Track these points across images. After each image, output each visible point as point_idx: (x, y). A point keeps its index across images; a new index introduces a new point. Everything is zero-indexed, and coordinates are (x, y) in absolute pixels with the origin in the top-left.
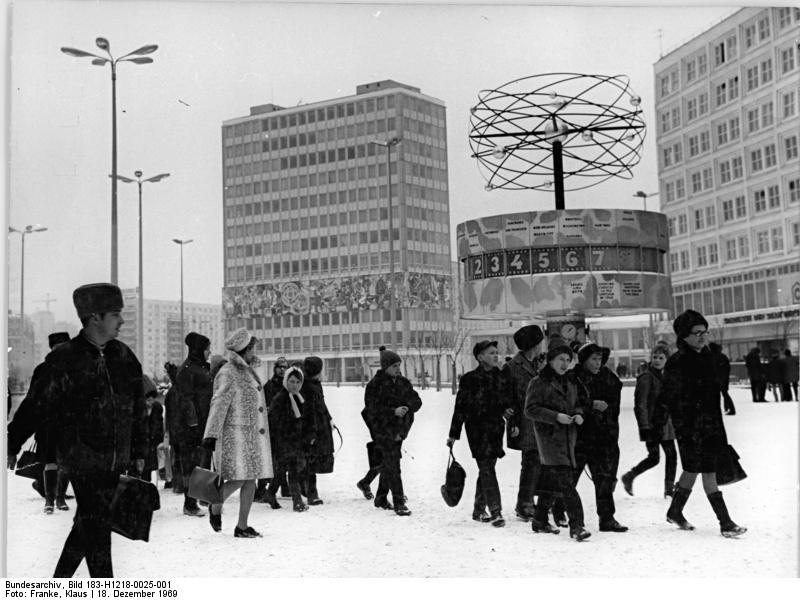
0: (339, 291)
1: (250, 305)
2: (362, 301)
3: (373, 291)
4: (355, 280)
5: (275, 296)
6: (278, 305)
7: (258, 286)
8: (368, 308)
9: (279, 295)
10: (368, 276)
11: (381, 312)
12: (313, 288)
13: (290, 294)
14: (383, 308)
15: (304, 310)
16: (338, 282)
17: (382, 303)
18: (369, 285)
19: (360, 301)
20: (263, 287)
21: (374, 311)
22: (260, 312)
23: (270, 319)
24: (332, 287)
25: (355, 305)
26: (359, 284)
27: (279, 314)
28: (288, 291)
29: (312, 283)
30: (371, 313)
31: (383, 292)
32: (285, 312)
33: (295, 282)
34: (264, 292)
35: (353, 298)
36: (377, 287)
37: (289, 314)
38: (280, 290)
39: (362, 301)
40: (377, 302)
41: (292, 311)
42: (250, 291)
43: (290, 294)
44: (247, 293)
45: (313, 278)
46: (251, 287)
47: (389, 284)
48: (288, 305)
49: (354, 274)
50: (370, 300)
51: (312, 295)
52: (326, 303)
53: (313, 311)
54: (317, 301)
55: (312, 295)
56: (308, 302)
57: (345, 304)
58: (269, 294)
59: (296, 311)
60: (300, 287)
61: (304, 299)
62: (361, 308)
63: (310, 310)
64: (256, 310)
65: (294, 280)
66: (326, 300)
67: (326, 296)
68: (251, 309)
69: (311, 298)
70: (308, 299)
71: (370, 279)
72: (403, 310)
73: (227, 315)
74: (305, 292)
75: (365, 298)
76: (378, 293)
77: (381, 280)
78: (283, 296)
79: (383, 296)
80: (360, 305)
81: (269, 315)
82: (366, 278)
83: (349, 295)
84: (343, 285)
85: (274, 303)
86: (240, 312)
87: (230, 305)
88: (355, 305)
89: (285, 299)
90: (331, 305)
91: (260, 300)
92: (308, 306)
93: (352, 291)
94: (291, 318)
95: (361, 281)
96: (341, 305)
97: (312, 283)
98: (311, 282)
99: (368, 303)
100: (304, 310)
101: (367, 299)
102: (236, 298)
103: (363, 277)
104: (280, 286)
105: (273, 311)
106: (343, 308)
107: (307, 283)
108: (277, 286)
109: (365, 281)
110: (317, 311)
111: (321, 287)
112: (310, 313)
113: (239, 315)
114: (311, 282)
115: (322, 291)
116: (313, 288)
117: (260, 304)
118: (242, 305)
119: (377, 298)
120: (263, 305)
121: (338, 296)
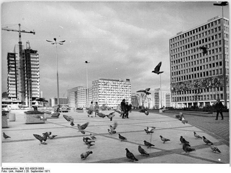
2: (210, 85)
5: (184, 85)
6: (185, 88)
7: (180, 83)
9: (185, 85)
12: (195, 82)
13: (188, 84)
17: (216, 85)
20: (181, 83)
22: (180, 90)
27: (185, 90)
31: (217, 82)
32: (187, 90)
33: (189, 81)
35: (207, 84)
36: (215, 80)
39: (210, 85)
42: (177, 84)
43: (188, 84)
47: (219, 79)
48: (188, 87)
51: (195, 84)
52: (199, 86)
54: (196, 86)
55: (195, 84)
56: (193, 86)
57: (204, 86)
62: (209, 87)
64: (179, 89)
67: (199, 84)
69: (194, 85)
71: (212, 78)
75: (211, 84)
77: (216, 78)
80: (209, 86)
81: (183, 90)
83: (206, 83)
84: (204, 81)
86: (175, 90)
87: (172, 88)
88: (208, 87)
89: (187, 86)
91: (180, 86)
95: (209, 79)
96: (203, 87)
98: (194, 80)
99: (212, 86)
102: (174, 86)
105: (184, 89)
107: (193, 81)
109: (211, 79)
110: (196, 89)
111: (197, 82)
115: (197, 83)
119: (215, 84)
120: (181, 88)
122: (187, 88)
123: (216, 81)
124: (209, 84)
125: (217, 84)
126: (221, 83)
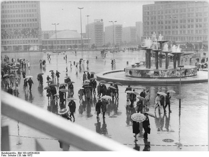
2: (28, 33)
3: (31, 31)
6: (5, 34)
8: (30, 35)
10: (30, 28)
11: (33, 36)
12: (15, 30)
16: (22, 29)
17: (33, 34)
18: (30, 30)
24: (20, 30)
25: (26, 34)
26: (27, 30)
29: (14, 29)
31: (33, 32)
32: (7, 35)
33: (10, 29)
36: (32, 31)
37: (8, 36)
39: (28, 33)
41: (9, 35)
45: (15, 28)
49: (26, 28)
51: (15, 32)
52: (18, 34)
53: (15, 35)
54: (16, 33)
55: (15, 32)
57: (23, 34)
61: (12, 33)
63: (14, 35)
66: (18, 33)
67: (18, 32)
71: (30, 29)
72: (38, 36)
74: (13, 31)
77: (33, 29)
83: (24, 32)
85: (4, 33)
88: (26, 34)
92: (13, 34)
93: (25, 31)
94: (9, 37)
95: (28, 29)
96: (22, 34)
97: (14, 29)
101: (29, 33)
103: (28, 28)
104: (6, 30)
106: (23, 35)
107: (13, 29)
108: (5, 30)
110: (16, 35)
111: (17, 30)
116: (15, 30)
124: (27, 33)
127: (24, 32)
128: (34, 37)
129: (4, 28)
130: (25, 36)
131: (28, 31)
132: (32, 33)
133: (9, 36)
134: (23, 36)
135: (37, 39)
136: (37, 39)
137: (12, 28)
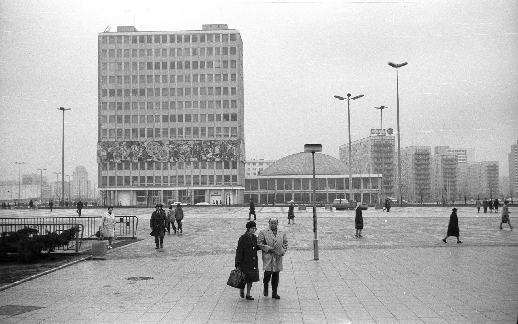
0: (192, 149)
1: (121, 154)
2: (209, 156)
3: (217, 150)
4: (204, 143)
5: (142, 149)
6: (144, 155)
7: (127, 142)
9: (145, 149)
10: (215, 140)
11: (223, 163)
12: (172, 146)
14: (224, 160)
15: (165, 159)
16: (192, 143)
17: (224, 157)
18: (215, 146)
19: (208, 156)
20: (130, 144)
21: (217, 162)
22: (129, 159)
23: (137, 163)
24: (187, 146)
25: (204, 158)
28: (152, 147)
30: (215, 163)
31: (225, 151)
32: (149, 160)
34: (132, 146)
35: (203, 154)
36: (221, 147)
37: (153, 161)
38: (145, 146)
39: (209, 156)
40: (220, 156)
41: (155, 159)
42: (120, 145)
43: (153, 149)
44: (118, 146)
45: (171, 140)
46: (122, 142)
47: (230, 147)
48: (153, 156)
49: (204, 139)
50: (216, 156)
51: (171, 150)
52: (182, 156)
53: (172, 160)
54: (175, 154)
55: (171, 150)
56: (168, 155)
57: (197, 157)
58: (136, 148)
59: (158, 159)
60: (161, 145)
61: (164, 152)
62: (209, 160)
65: (156, 140)
66: (182, 154)
68: (121, 157)
70: (168, 152)
73: (101, 160)
74: (166, 149)
75: (212, 154)
76: (221, 151)
77: (224, 144)
78: (148, 150)
79: (225, 154)
80: (208, 158)
81: (136, 161)
82: (213, 142)
83: (199, 151)
85: (140, 154)
87: (104, 153)
88: (204, 158)
89: (150, 152)
90: (185, 157)
92: (168, 157)
93: (202, 149)
94: (154, 164)
95: (209, 144)
96: (193, 157)
99: (214, 157)
100: (165, 159)
101: (213, 155)
102: (109, 149)
103: (211, 141)
105: (140, 159)
107: (168, 143)
108: (143, 143)
109: (211, 143)
110: (174, 160)
111: (179, 145)
112: (169, 161)
113: (112, 160)
114: (170, 142)
116: (172, 146)
117: (128, 154)
118: (114, 154)
119: (221, 155)
120: (131, 155)
121: (191, 152)
122: (149, 156)
123: (223, 149)
124: (208, 153)
125: (227, 155)
126: (235, 154)
127: (199, 151)
128: (227, 166)
129: (142, 139)
130: (200, 163)
131: (210, 150)
132: (221, 155)
133: (154, 161)
134: (194, 162)
135: (235, 172)
136: (235, 172)
137: (165, 139)
